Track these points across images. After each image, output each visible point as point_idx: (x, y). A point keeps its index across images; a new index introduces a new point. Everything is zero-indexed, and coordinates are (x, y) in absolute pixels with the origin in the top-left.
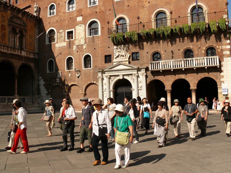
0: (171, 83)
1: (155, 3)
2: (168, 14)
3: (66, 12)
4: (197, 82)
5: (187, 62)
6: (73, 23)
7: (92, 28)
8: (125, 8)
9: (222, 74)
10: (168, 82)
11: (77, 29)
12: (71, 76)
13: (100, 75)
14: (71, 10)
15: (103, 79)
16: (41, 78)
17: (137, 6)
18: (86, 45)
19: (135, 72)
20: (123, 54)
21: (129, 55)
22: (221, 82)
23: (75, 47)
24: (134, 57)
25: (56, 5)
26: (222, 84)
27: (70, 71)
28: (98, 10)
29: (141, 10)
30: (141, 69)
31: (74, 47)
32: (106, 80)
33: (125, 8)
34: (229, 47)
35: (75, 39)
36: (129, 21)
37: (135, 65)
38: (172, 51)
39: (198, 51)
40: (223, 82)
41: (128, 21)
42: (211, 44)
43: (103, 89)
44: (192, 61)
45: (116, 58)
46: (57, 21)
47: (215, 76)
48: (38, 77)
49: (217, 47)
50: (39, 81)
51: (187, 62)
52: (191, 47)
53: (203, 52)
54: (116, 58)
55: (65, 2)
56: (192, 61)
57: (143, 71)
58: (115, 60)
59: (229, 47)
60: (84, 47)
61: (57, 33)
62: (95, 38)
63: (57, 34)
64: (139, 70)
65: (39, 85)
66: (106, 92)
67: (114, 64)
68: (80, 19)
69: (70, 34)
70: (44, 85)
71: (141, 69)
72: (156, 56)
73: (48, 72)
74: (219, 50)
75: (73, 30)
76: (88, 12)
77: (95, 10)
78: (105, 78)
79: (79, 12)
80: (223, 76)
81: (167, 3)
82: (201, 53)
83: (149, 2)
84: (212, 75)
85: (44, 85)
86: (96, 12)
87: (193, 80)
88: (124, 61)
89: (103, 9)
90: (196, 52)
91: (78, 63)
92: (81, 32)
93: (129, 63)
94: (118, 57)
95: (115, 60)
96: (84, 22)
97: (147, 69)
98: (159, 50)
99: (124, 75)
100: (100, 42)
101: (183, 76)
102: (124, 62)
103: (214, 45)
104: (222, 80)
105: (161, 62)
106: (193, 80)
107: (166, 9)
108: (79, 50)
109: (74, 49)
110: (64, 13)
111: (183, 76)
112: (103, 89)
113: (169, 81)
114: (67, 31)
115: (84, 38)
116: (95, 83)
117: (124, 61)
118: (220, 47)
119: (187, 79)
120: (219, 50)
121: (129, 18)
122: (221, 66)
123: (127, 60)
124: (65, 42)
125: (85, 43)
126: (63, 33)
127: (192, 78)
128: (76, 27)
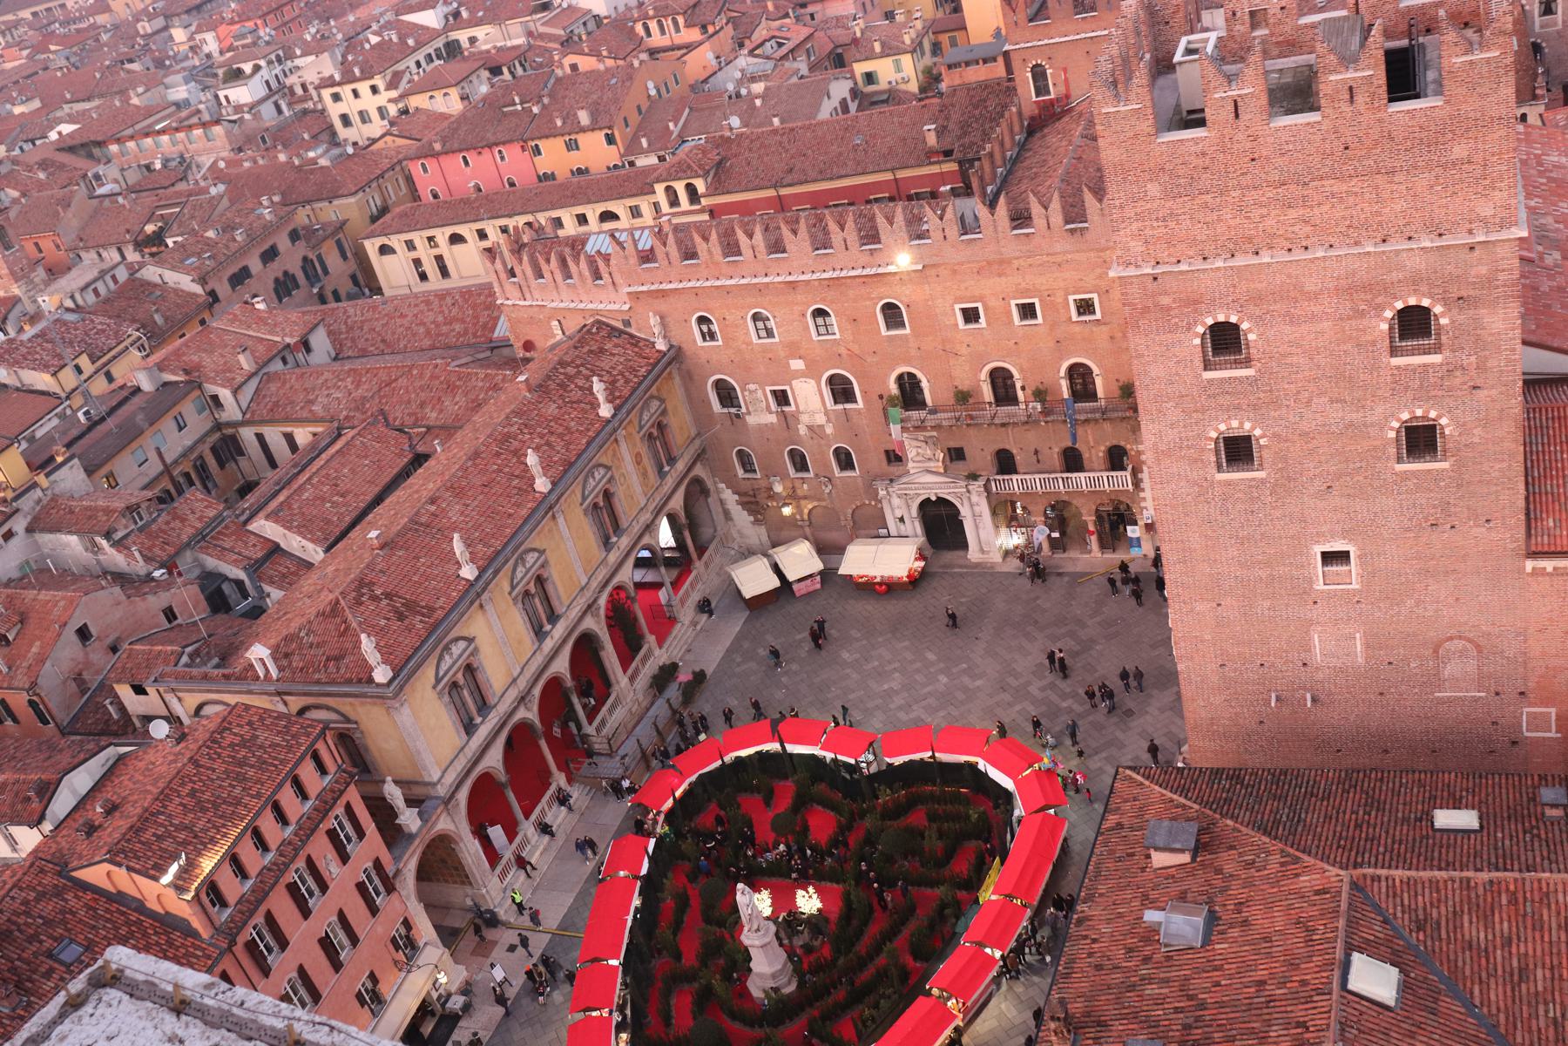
9: (1142, 495)
22: (1142, 509)
23: (802, 430)
28: (843, 351)
33: (913, 352)
41: (925, 384)
50: (718, 492)
60: (829, 430)
61: (743, 390)
65: (722, 502)
68: (797, 364)
69: (782, 398)
85: (738, 503)
89: (856, 348)
92: (810, 397)
95: (910, 465)
96: (812, 372)
97: (987, 487)
105: (1014, 477)
114: (768, 389)
125: (829, 420)
126: (760, 393)
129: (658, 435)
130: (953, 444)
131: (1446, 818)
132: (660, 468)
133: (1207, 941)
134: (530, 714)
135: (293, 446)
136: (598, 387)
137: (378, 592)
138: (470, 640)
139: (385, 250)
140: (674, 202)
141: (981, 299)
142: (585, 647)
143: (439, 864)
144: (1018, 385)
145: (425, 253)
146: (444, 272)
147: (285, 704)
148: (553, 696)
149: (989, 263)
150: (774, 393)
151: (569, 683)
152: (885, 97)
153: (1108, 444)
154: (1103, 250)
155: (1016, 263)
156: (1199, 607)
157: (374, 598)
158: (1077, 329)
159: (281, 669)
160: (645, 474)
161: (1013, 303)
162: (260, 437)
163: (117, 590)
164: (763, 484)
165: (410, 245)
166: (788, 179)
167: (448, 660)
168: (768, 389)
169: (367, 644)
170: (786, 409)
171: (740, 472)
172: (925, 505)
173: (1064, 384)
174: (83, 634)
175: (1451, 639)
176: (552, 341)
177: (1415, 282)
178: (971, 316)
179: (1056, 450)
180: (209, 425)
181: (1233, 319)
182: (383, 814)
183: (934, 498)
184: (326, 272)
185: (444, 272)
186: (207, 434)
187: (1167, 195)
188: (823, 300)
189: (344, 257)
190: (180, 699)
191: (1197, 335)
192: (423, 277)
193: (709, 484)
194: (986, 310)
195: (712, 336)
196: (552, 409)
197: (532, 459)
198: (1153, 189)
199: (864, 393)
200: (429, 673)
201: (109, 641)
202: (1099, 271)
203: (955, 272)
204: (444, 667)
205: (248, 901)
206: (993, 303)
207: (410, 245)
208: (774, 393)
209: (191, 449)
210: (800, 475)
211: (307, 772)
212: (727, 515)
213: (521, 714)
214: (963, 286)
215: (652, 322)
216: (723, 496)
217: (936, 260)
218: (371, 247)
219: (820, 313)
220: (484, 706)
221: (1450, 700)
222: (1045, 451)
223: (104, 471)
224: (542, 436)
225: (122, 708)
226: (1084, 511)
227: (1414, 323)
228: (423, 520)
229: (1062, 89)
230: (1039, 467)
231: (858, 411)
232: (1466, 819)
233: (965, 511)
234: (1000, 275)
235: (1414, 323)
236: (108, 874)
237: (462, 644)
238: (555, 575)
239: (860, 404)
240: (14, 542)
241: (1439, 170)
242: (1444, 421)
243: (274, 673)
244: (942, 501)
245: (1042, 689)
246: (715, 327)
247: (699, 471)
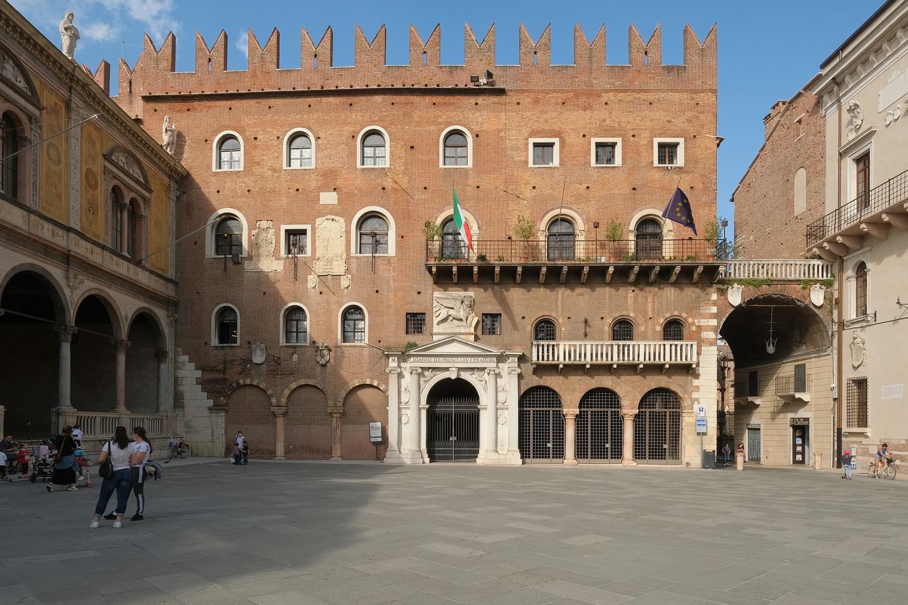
1: (550, 191)
2: (580, 225)
3: (281, 169)
5: (626, 349)
6: (316, 212)
8: (470, 190)
9: (696, 382)
10: (571, 394)
11: (322, 227)
12: (299, 361)
13: (393, 363)
14: (295, 165)
15: (400, 375)
16: (186, 358)
17: (502, 193)
18: (349, 276)
19: (491, 364)
20: (462, 314)
21: (476, 319)
22: (693, 401)
23: (312, 281)
24: (489, 324)
25: (246, 140)
26: (696, 407)
27: (294, 347)
28: (388, 183)
29: (512, 206)
30: (508, 356)
31: (310, 277)
32: (408, 380)
33: (470, 190)
34: (714, 322)
35: (314, 257)
36: (479, 228)
37: (490, 344)
38: (586, 322)
39: (646, 327)
40: (697, 400)
42: (676, 313)
43: (400, 403)
44: (636, 348)
45: (438, 323)
46: (249, 191)
47: (682, 386)
48: (176, 355)
49: (690, 320)
50: (176, 368)
51: (626, 349)
52: (632, 314)
53: (659, 328)
54: (438, 323)
55: (278, 138)
56: (636, 348)
57: (512, 363)
58: (439, 330)
59: (714, 322)
60: (345, 282)
62: (379, 261)
63: (250, 232)
64: (501, 358)
65: (176, 381)
66: (408, 412)
67: (435, 338)
68: (329, 198)
70: (199, 381)
71: (508, 356)
73: (214, 341)
74: (694, 328)
75: (308, 227)
76: (357, 183)
77: (379, 181)
78: (407, 374)
79: (329, 178)
80: (697, 388)
81: (580, 199)
83: (534, 187)
84: (673, 383)
85: (199, 381)
86: (383, 189)
87: (630, 394)
88: (464, 334)
89: (404, 182)
90: (640, 328)
91: (323, 327)
93: (477, 338)
94: (445, 320)
96: (342, 210)
98: (554, 315)
99: (460, 369)
100: (392, 273)
101: (606, 381)
102: (463, 336)
103: (684, 315)
104: (695, 395)
106: (630, 394)
107: (576, 211)
108: (325, 290)
109: (310, 285)
110: (274, 170)
111: (606, 381)
112: (400, 403)
113: (574, 390)
114: (284, 227)
115: (344, 256)
116: (375, 384)
117: (464, 334)
118: (696, 321)
119: (617, 390)
120: (694, 328)
121: (477, 222)
122: (698, 364)
123: (472, 330)
125: (348, 271)
126: (271, 231)
127: (629, 388)
128: (318, 221)
141: (558, 134)
149: (577, 95)
154: (696, 92)
155: (605, 97)
158: (657, 175)
179: (609, 320)
188: (381, 121)
193: (170, 346)
194: (563, 144)
202: (689, 114)
203: (536, 101)
206: (573, 139)
212: (178, 401)
214: (543, 117)
215: (165, 126)
216: (181, 374)
217: (522, 85)
222: (595, 322)
226: (624, 402)
231: (389, 260)
233: (486, 399)
244: (460, 382)
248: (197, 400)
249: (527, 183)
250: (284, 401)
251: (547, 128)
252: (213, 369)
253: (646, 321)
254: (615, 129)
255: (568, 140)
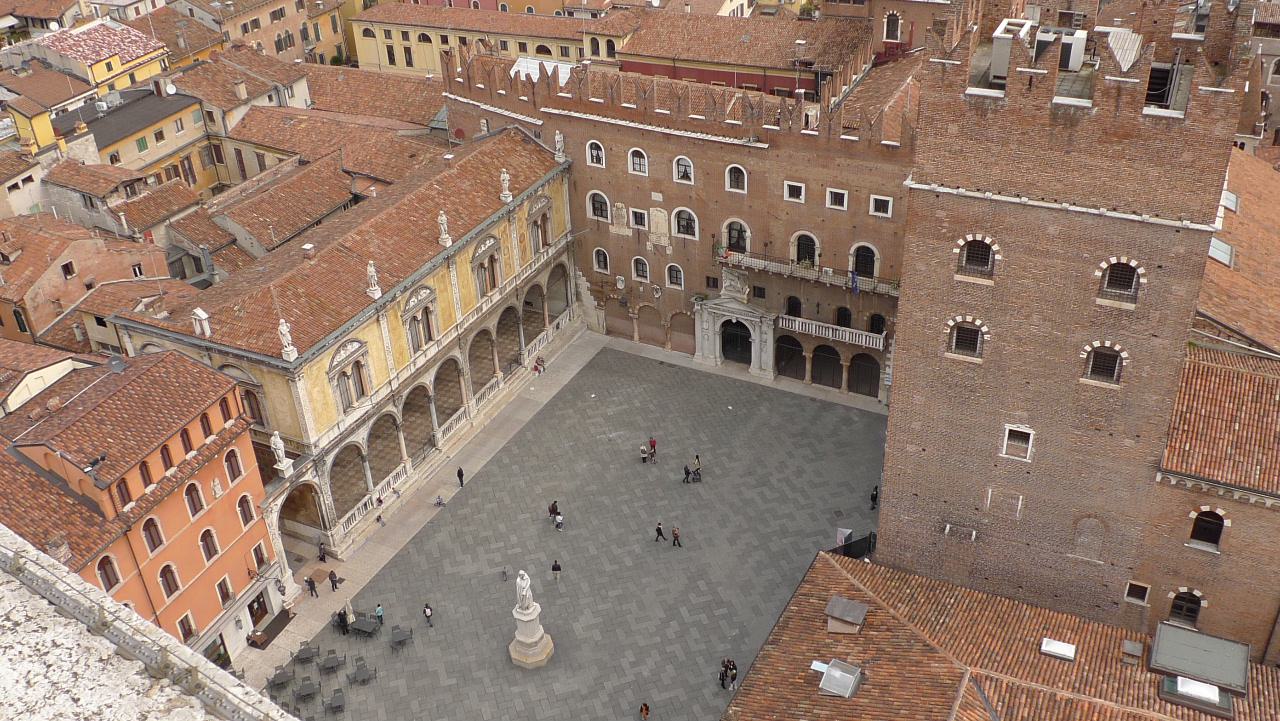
0: (813, 347)
4: (851, 356)
7: (686, 226)
9: (888, 355)
22: (886, 366)
23: (649, 246)
28: (694, 196)
52: (848, 307)
53: (865, 318)
61: (612, 206)
68: (657, 197)
69: (639, 219)
72: (794, 308)
80: (889, 359)
82: (863, 320)
85: (591, 291)
86: (690, 197)
92: (661, 223)
93: (749, 301)
96: (667, 205)
97: (776, 321)
98: (798, 296)
104: (887, 363)
109: (648, 248)
114: (631, 210)
124: (629, 228)
129: (541, 223)
130: (757, 284)
131: (1051, 646)
132: (537, 251)
133: (855, 694)
134: (396, 410)
135: (262, 167)
136: (505, 177)
137: (301, 291)
138: (362, 344)
139: (367, 33)
140: (596, 51)
142: (448, 371)
143: (300, 503)
144: (817, 253)
145: (397, 42)
146: (409, 63)
147: (210, 359)
148: (415, 400)
150: (635, 213)
151: (431, 392)
152: (773, 11)
153: (873, 312)
156: (910, 448)
157: (297, 296)
158: (871, 221)
159: (213, 331)
160: (524, 251)
161: (829, 190)
162: (238, 153)
163: (100, 242)
164: (610, 279)
165: (388, 34)
166: (684, 57)
167: (343, 354)
168: (631, 210)
169: (284, 328)
170: (641, 227)
171: (596, 267)
172: (727, 324)
173: (851, 260)
174: (67, 269)
175: (1089, 516)
176: (478, 135)
177: (1130, 247)
178: (795, 192)
179: (834, 307)
180: (200, 134)
181: (988, 241)
182: (266, 459)
183: (734, 321)
184: (318, 39)
185: (409, 63)
186: (199, 140)
187: (962, 133)
189: (335, 31)
190: (130, 336)
191: (958, 246)
192: (392, 60)
195: (599, 160)
196: (466, 185)
197: (443, 219)
198: (953, 129)
199: (702, 230)
200: (325, 361)
201: (87, 280)
202: (897, 181)
204: (338, 359)
205: (147, 500)
206: (813, 185)
207: (388, 34)
208: (635, 213)
209: (181, 149)
210: (639, 279)
211: (215, 415)
213: (390, 408)
214: (794, 168)
216: (579, 282)
218: (357, 31)
219: (637, 154)
220: (362, 393)
221: (1076, 562)
223: (111, 150)
224: (454, 203)
225: (85, 334)
227: (1121, 276)
228: (348, 245)
229: (906, 38)
230: (817, 316)
232: (1067, 650)
233: (755, 336)
234: (824, 167)
235: (1121, 276)
236: (46, 455)
237: (356, 345)
238: (437, 309)
239: (697, 238)
240: (30, 185)
241: (1168, 167)
242: (1124, 355)
243: (208, 333)
244: (738, 322)
245: (779, 480)
246: (603, 154)
247: (564, 258)
248: (588, 299)
249: (782, 210)
250: (636, 312)
251: (797, 175)
252: (596, 284)
253: (858, 312)
254: (842, 183)
255: (811, 186)
